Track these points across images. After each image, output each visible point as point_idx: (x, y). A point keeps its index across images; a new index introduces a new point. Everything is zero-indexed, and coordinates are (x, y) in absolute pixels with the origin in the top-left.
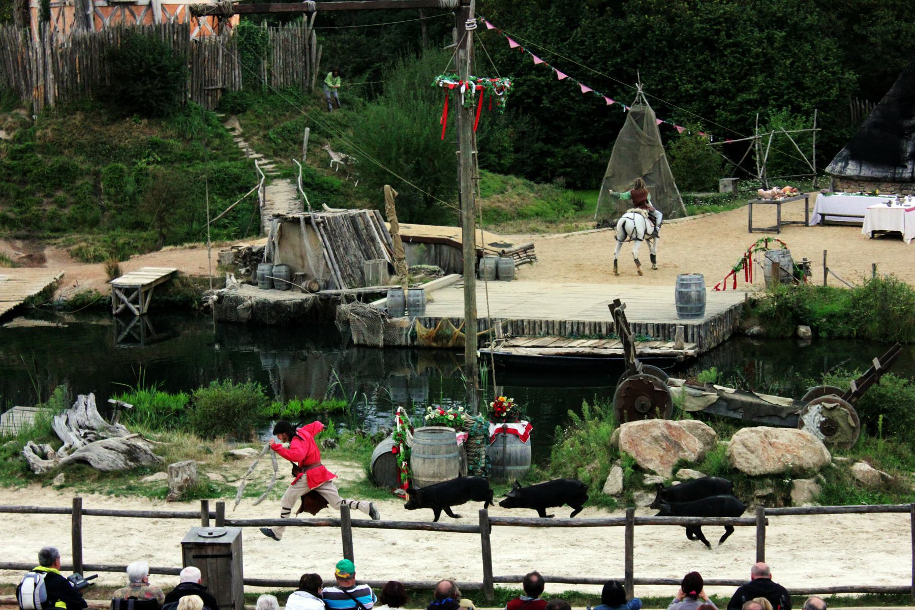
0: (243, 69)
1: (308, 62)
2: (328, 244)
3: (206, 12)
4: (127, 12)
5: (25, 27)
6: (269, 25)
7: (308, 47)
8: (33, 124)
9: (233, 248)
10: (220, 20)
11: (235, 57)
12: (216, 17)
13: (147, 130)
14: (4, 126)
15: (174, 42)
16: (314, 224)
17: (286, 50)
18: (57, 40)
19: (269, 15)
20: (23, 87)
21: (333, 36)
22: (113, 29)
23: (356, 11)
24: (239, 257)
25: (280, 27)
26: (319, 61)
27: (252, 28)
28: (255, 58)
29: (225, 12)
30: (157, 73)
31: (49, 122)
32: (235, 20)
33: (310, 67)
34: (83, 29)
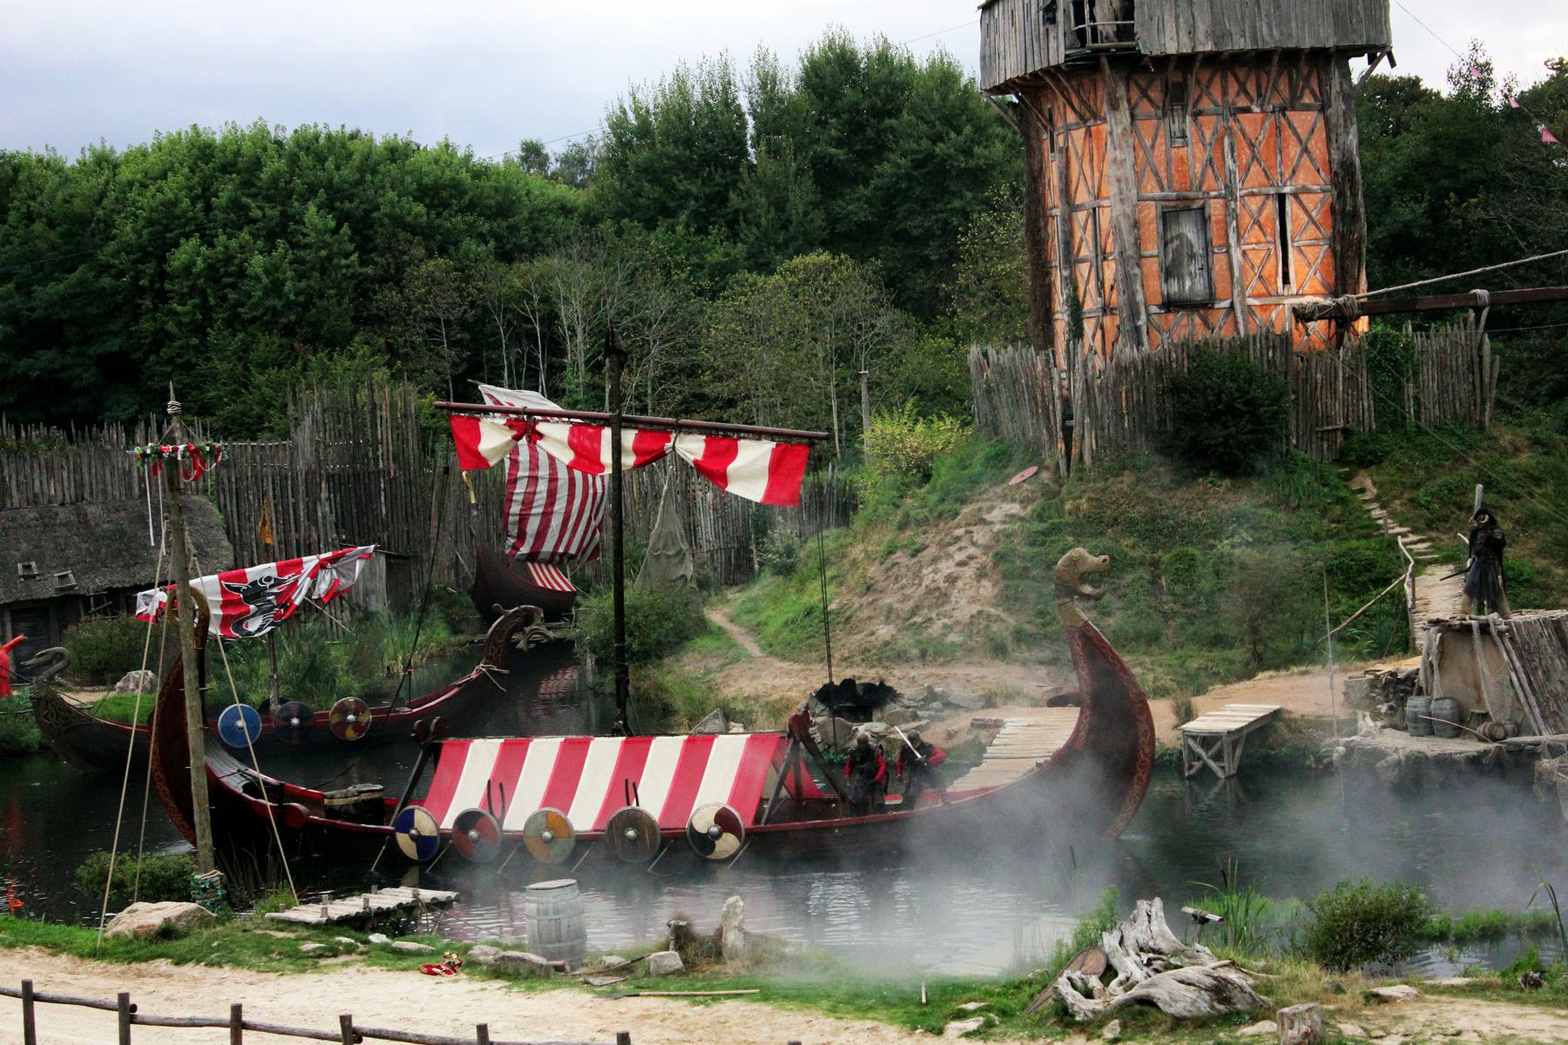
0: (1377, 399)
1: (1477, 382)
2: (1518, 664)
3: (1317, 315)
4: (1197, 320)
5: (1046, 348)
6: (1414, 330)
7: (1476, 360)
8: (1059, 493)
9: (1366, 672)
10: (1339, 326)
11: (1364, 380)
12: (1333, 323)
13: (1230, 496)
14: (1017, 496)
15: (1268, 361)
16: (1494, 632)
17: (1442, 367)
18: (1094, 367)
19: (1412, 312)
20: (1045, 437)
21: (1516, 341)
22: (1176, 346)
23: (1552, 302)
24: (1376, 687)
25: (1432, 332)
26: (1495, 381)
27: (1389, 335)
28: (1395, 381)
29: (1347, 313)
30: (1243, 408)
31: (1083, 487)
32: (1362, 324)
33: (1482, 391)
34: (1132, 347)
